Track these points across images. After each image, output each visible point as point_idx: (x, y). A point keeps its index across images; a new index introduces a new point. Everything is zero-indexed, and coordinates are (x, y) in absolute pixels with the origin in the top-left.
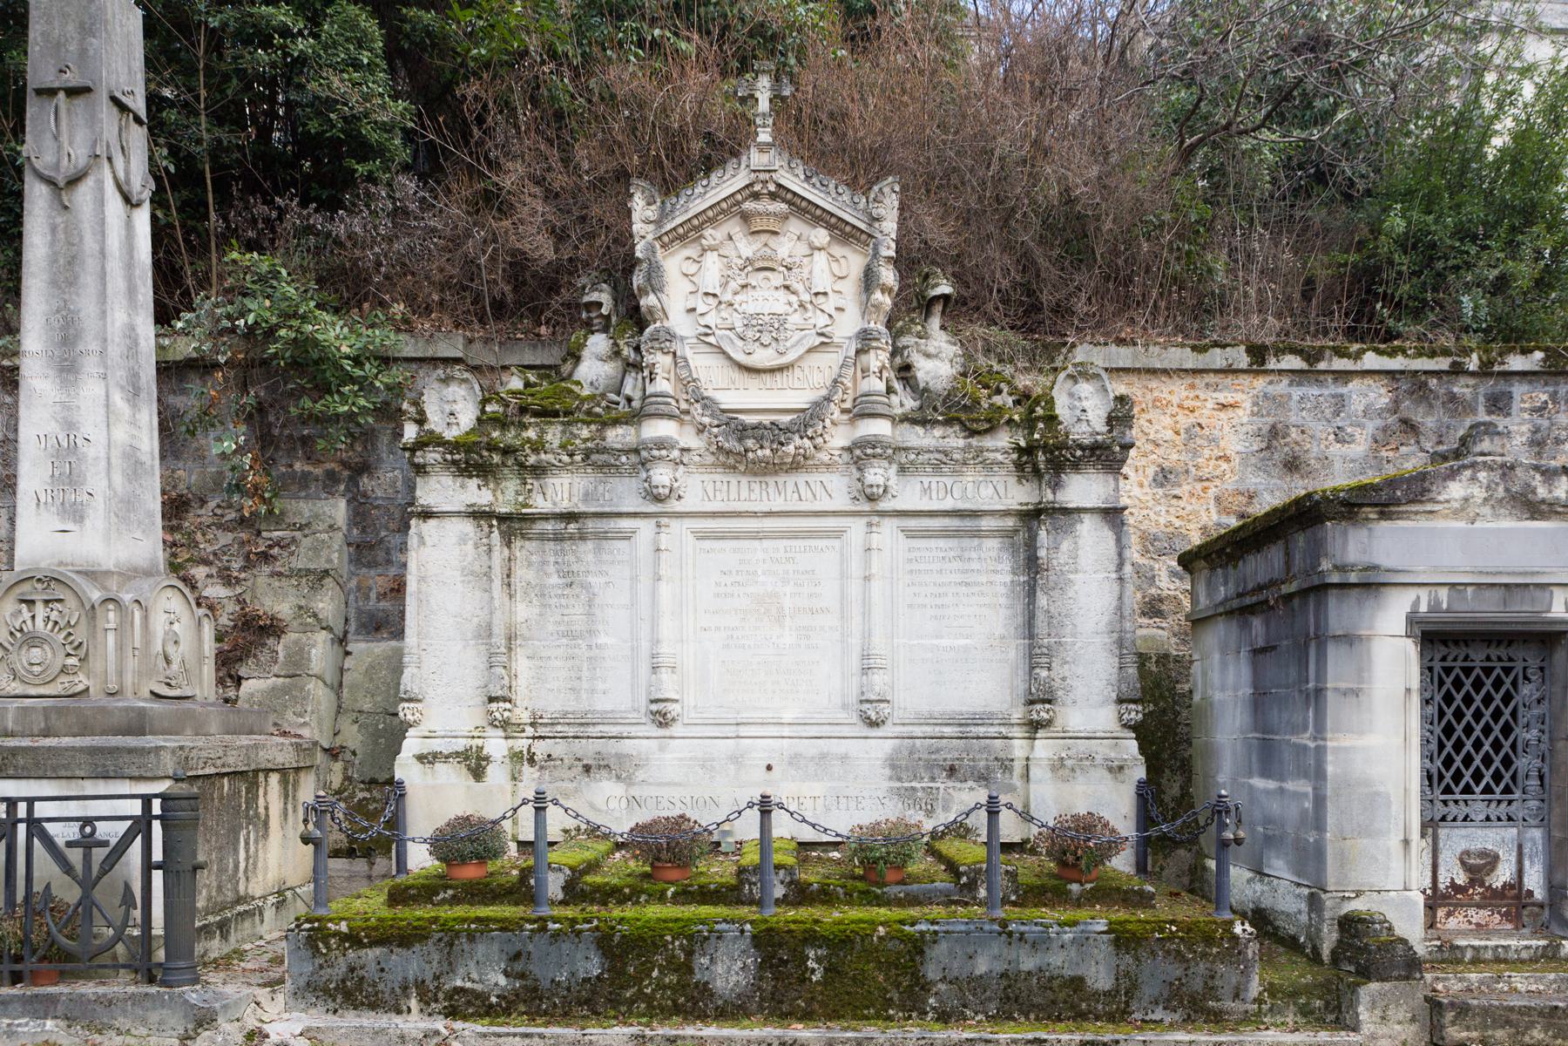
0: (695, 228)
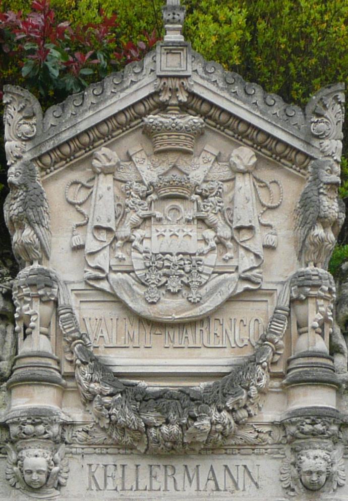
0: (85, 146)
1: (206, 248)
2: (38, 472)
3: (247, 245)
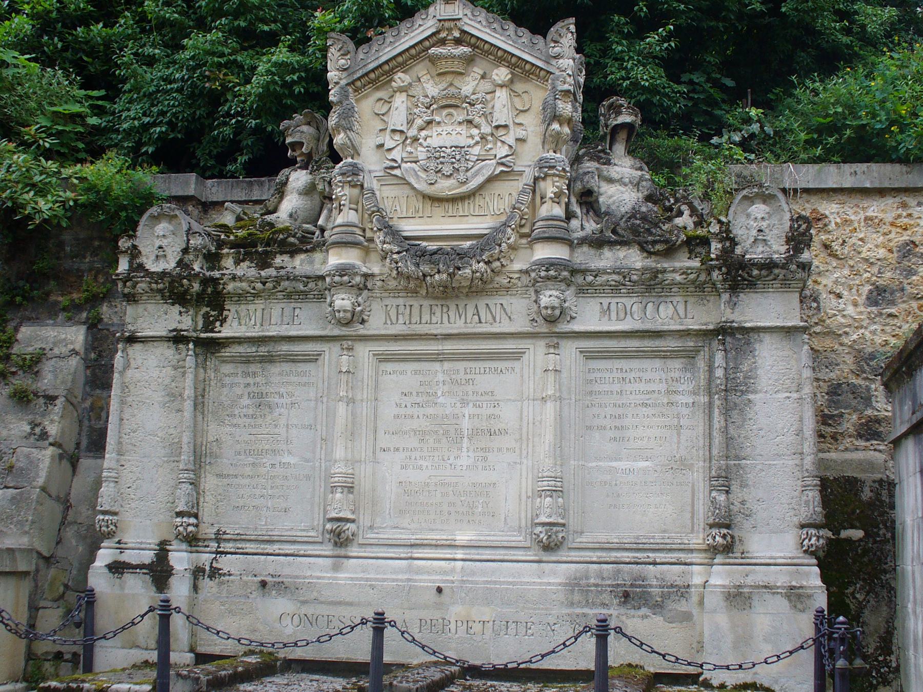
1: (472, 142)
2: (345, 311)
3: (503, 139)
